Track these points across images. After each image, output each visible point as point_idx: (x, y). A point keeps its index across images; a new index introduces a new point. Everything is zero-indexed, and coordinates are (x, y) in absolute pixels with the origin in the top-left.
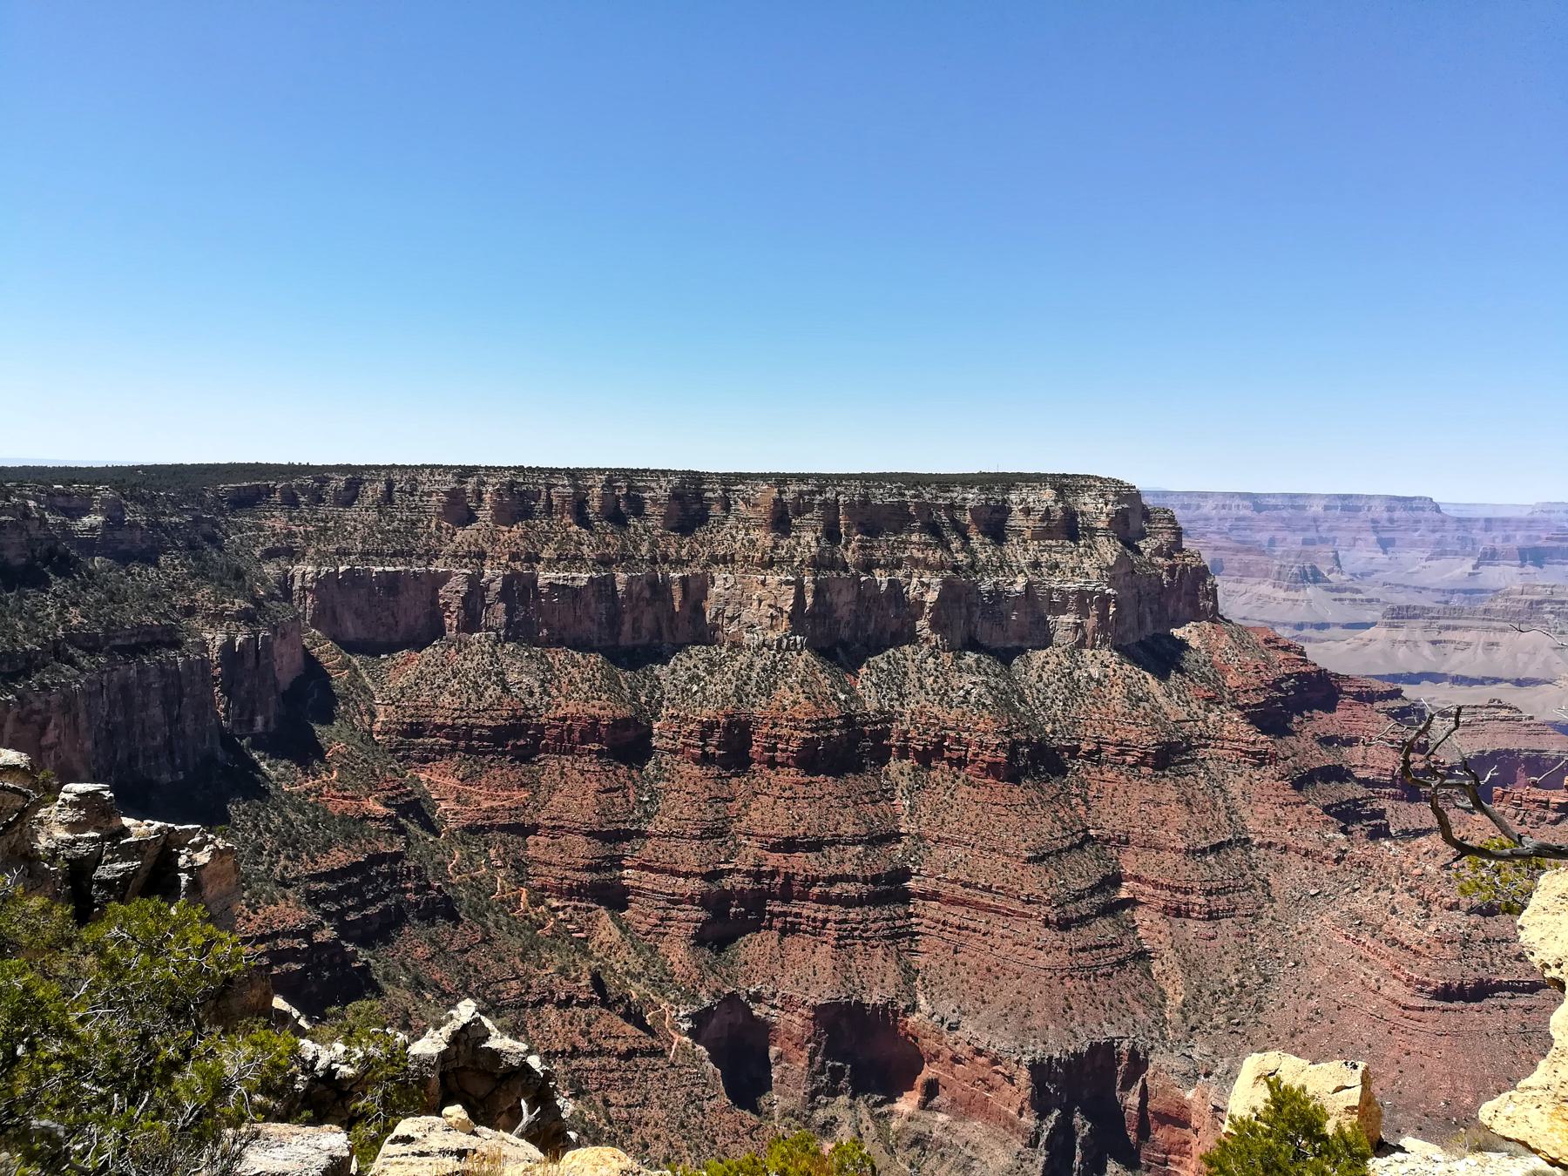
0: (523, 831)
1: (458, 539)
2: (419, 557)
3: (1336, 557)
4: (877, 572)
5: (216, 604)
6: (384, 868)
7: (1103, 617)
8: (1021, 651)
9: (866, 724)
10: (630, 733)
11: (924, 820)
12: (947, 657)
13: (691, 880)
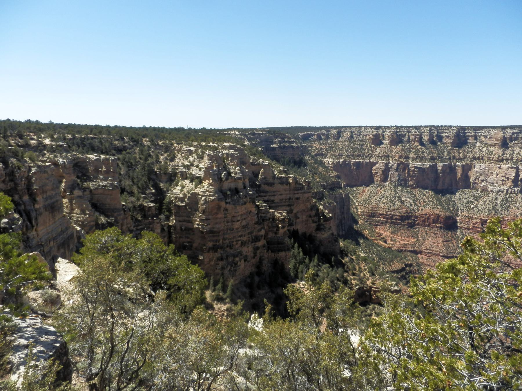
1: (378, 150)
2: (366, 157)
10: (450, 221)
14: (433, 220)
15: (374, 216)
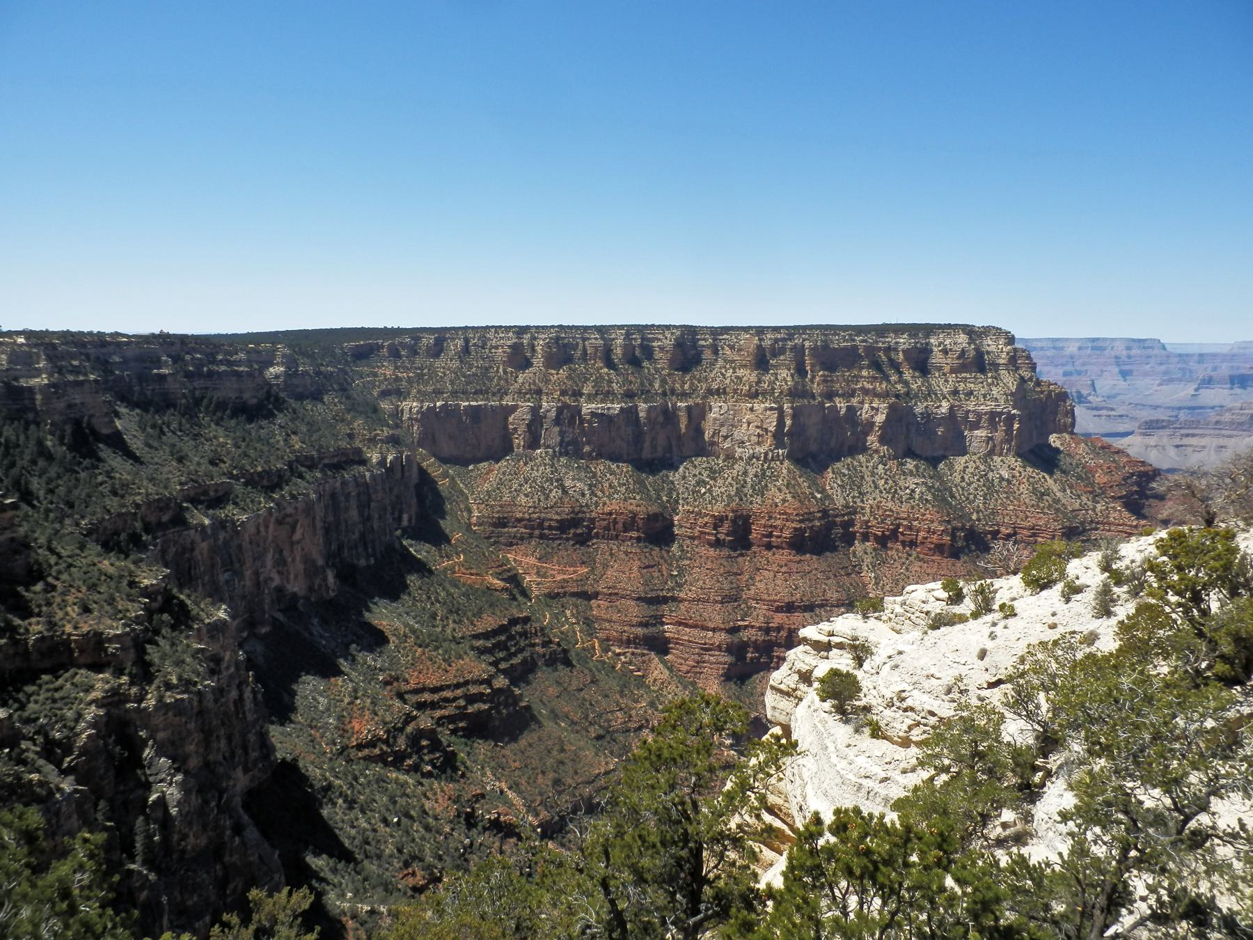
0: (587, 596)
1: (520, 380)
2: (494, 394)
3: (1093, 385)
4: (837, 400)
5: (370, 431)
6: (518, 628)
7: (1009, 430)
8: (945, 457)
9: (837, 516)
10: (659, 525)
11: (887, 587)
12: (893, 464)
13: (718, 634)
14: (624, 523)
15: (505, 526)
